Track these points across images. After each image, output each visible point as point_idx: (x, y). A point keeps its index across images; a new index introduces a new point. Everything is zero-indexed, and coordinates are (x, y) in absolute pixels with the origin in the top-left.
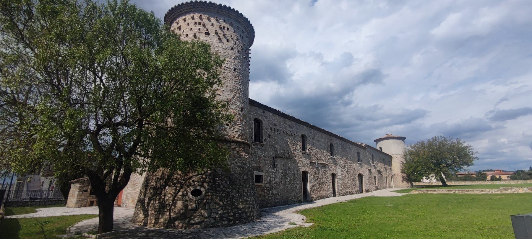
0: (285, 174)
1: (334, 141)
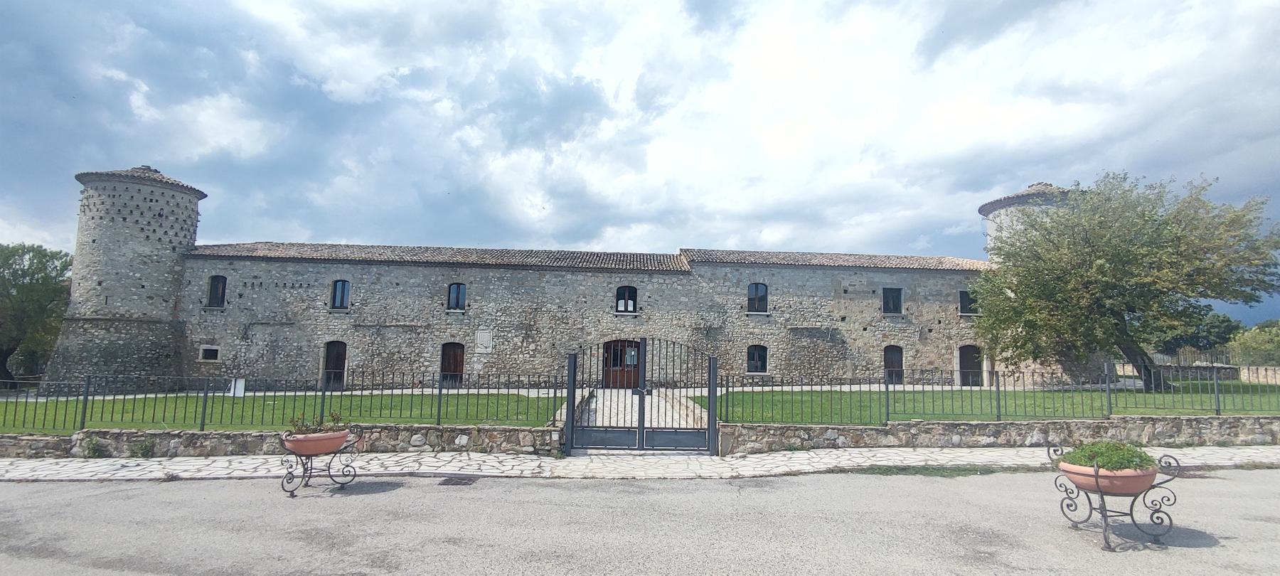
0: (273, 347)
1: (465, 276)
